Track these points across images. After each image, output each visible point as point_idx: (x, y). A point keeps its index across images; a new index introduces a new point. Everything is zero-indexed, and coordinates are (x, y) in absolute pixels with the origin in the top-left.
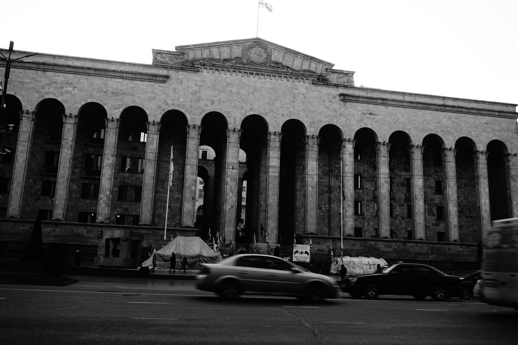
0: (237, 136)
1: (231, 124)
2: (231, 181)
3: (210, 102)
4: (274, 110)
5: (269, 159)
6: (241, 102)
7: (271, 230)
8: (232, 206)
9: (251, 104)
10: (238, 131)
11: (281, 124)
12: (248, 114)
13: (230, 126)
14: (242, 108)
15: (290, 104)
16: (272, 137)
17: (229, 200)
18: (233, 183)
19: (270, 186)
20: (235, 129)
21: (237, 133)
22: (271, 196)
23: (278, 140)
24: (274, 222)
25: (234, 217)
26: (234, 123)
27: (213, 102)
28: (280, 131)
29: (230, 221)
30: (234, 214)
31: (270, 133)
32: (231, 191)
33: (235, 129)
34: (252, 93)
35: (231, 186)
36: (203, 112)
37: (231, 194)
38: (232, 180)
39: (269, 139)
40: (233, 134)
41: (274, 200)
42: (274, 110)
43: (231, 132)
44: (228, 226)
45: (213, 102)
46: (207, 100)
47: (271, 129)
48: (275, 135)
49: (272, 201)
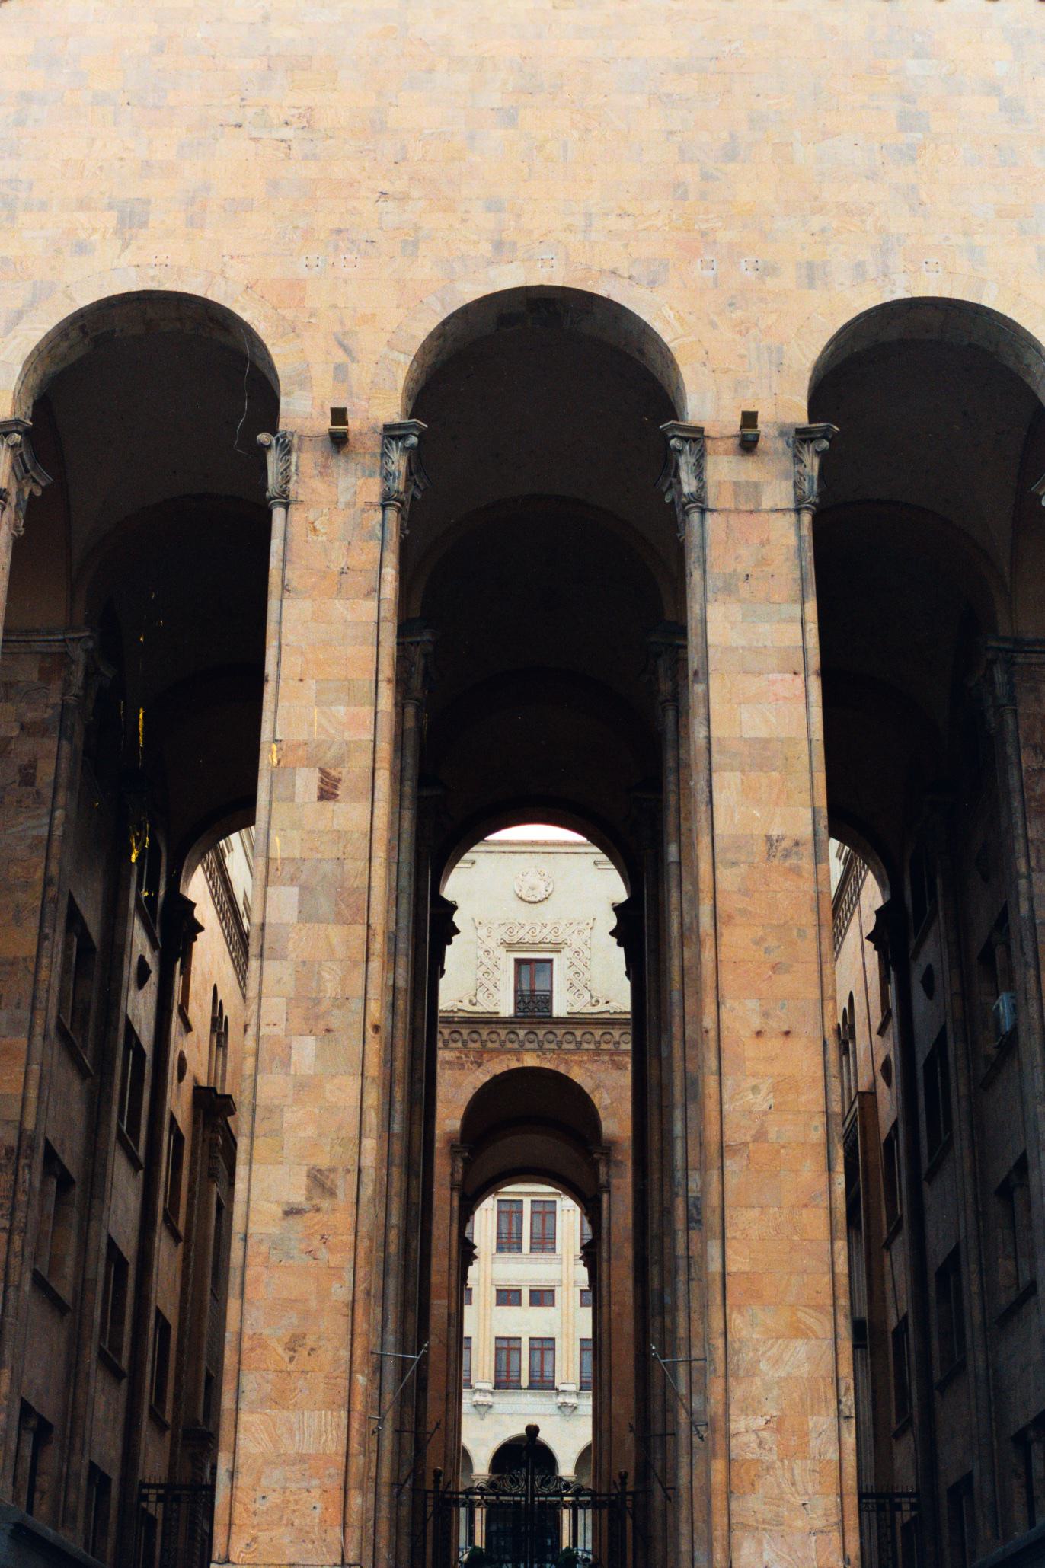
0: (374, 490)
1: (304, 381)
2: (306, 915)
3: (111, 219)
4: (725, 236)
5: (703, 675)
6: (404, 198)
7: (777, 1425)
8: (320, 1182)
9: (494, 206)
10: (373, 443)
11: (805, 353)
12: (471, 291)
13: (301, 409)
14: (411, 247)
15: (872, 176)
16: (724, 470)
17: (291, 1117)
18: (336, 934)
19: (737, 940)
20: (339, 415)
21: (371, 461)
22: (751, 1050)
23: (779, 492)
24: (798, 1331)
25: (341, 1292)
26: (340, 373)
27: (131, 221)
28: (799, 414)
29: (294, 1344)
30: (342, 1259)
31: (697, 437)
32: (312, 1015)
33: (339, 415)
34: (509, 117)
35: (307, 970)
36: (32, 304)
37: (306, 1051)
38: (325, 905)
39: (688, 484)
40: (324, 471)
41: (783, 1085)
42: (725, 236)
43: (305, 461)
44: (280, 1399)
45: (131, 221)
46: (83, 205)
47: (706, 401)
48: (748, 445)
49: (761, 1101)
